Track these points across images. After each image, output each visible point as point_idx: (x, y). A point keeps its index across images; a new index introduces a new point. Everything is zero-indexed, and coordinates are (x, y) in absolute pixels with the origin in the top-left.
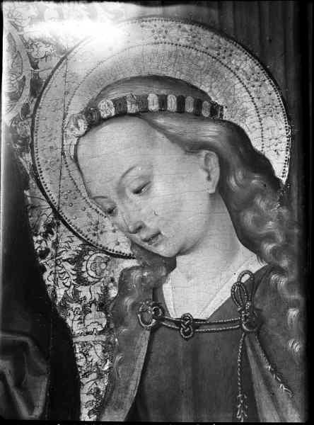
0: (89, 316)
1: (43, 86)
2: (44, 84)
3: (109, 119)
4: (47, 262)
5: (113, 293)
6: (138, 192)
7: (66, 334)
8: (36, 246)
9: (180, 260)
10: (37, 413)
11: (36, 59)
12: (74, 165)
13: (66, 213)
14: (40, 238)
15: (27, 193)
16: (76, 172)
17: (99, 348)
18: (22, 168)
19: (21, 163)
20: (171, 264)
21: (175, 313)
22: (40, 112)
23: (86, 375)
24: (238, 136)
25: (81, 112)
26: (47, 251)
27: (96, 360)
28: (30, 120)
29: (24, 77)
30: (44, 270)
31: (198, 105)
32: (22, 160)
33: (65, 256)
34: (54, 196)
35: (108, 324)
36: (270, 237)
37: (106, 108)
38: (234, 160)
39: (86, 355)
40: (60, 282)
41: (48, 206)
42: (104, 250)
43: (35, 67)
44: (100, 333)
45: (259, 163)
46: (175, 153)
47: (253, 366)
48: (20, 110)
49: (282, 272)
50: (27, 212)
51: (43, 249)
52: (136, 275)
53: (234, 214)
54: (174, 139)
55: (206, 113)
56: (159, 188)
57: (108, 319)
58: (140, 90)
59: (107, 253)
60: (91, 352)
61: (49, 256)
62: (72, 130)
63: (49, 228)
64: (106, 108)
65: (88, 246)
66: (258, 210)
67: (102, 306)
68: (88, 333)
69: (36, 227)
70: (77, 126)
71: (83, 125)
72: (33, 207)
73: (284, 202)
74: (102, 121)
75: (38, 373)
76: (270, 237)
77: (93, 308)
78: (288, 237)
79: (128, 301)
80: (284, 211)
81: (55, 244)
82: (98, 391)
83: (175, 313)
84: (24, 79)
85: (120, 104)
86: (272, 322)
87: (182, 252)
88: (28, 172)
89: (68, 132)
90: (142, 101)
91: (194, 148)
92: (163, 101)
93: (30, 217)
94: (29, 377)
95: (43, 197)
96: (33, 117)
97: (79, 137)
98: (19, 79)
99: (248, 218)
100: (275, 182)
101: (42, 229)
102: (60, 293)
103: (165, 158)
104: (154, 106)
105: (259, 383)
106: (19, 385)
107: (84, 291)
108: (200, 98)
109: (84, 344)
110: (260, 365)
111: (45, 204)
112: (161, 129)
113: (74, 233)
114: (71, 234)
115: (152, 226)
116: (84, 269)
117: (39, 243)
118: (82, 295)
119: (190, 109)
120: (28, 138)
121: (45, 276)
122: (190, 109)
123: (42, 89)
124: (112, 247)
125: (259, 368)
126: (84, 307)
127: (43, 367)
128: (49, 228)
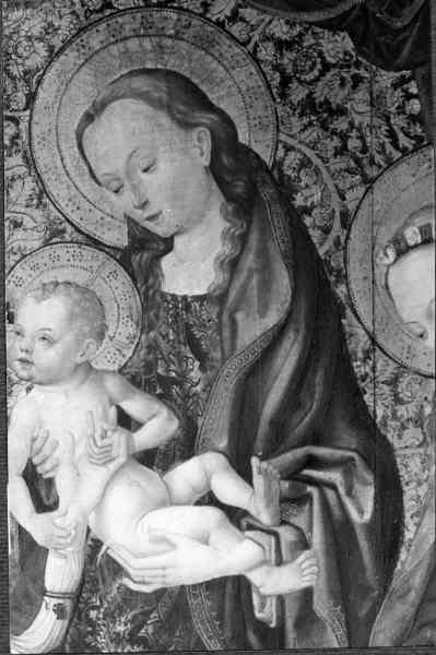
0: (407, 431)
3: (416, 246)
4: (366, 385)
7: (388, 448)
8: (356, 370)
10: (368, 516)
12: (385, 292)
13: (380, 340)
14: (359, 363)
15: (344, 321)
16: (389, 300)
17: (418, 460)
22: (350, 243)
23: (407, 484)
25: (389, 242)
26: (367, 375)
27: (416, 470)
30: (365, 392)
32: (338, 291)
33: (381, 379)
34: (369, 324)
35: (425, 438)
37: (412, 235)
39: (406, 466)
40: (379, 402)
42: (417, 373)
44: (419, 446)
48: (332, 243)
50: (345, 341)
57: (424, 434)
59: (421, 375)
60: (411, 464)
61: (369, 380)
62: (381, 259)
63: (367, 355)
64: (412, 235)
68: (406, 447)
69: (356, 354)
70: (386, 255)
71: (391, 253)
72: (351, 335)
74: (409, 248)
75: (366, 484)
77: (411, 425)
81: (374, 369)
82: (419, 497)
84: (333, 211)
88: (344, 302)
89: (378, 261)
94: (357, 487)
96: (345, 248)
97: (389, 266)
101: (360, 355)
102: (380, 413)
106: (349, 493)
107: (402, 411)
109: (405, 456)
113: (390, 358)
114: (386, 358)
116: (399, 390)
117: (360, 369)
118: (399, 414)
121: (366, 397)
126: (402, 424)
127: (370, 478)
128: (367, 357)
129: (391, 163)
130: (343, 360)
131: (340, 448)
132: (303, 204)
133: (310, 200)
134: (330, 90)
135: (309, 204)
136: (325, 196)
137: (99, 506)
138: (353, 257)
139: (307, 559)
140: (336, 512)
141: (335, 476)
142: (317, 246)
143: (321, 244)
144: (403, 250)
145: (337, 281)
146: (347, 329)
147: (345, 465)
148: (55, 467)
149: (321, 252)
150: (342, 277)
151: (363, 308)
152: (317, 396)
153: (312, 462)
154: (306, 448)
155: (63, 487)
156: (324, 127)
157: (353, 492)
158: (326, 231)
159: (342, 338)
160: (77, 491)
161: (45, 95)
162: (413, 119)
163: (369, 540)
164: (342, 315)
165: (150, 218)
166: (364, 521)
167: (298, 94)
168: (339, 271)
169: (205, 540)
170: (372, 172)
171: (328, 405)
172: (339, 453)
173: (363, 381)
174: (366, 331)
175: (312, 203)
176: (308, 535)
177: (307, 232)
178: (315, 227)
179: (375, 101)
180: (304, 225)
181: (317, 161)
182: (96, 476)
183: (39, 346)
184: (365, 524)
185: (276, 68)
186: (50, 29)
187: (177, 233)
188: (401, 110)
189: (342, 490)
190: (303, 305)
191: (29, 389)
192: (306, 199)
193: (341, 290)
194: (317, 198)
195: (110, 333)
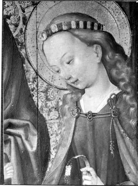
0: (51, 112)
1: (28, 20)
2: (28, 19)
3: (56, 32)
4: (34, 93)
5: (61, 103)
6: (69, 63)
7: (44, 120)
8: (30, 86)
9: (86, 90)
10: (35, 149)
11: (24, 8)
12: (42, 53)
13: (40, 73)
14: (31, 83)
15: (24, 65)
16: (44, 56)
17: (56, 125)
18: (22, 55)
19: (21, 53)
20: (83, 92)
21: (85, 110)
22: (27, 31)
23: (52, 135)
24: (110, 37)
25: (44, 30)
26: (34, 88)
27: (55, 129)
28: (23, 35)
29: (19, 16)
31: (92, 25)
32: (21, 52)
33: (41, 90)
34: (35, 66)
35: (59, 116)
36: (123, 80)
37: (54, 28)
38: (108, 48)
39: (51, 128)
40: (39, 100)
41: (33, 70)
42: (56, 87)
43: (24, 12)
44: (57, 119)
45: (118, 49)
46: (84, 46)
47: (117, 130)
48: (19, 31)
49: (128, 93)
50: (25, 73)
51: (32, 88)
52: (69, 97)
53: (108, 71)
54: (83, 40)
55: (96, 28)
56: (77, 61)
57: (59, 114)
58: (67, 19)
59: (58, 88)
60: (53, 127)
61: (35, 91)
62: (41, 38)
64: (54, 28)
65: (50, 85)
66: (118, 69)
67: (56, 109)
68: (51, 119)
69: (29, 79)
70: (42, 36)
71: (45, 36)
72: (27, 71)
73: (130, 65)
74: (52, 34)
75: (34, 135)
76: (123, 80)
77: (53, 110)
78: (130, 80)
79: (67, 107)
80: (129, 69)
81: (37, 86)
82: (57, 141)
83: (85, 110)
84: (19, 17)
85: (59, 26)
86: (124, 113)
87: (87, 87)
88: (24, 57)
89: (39, 39)
90: (69, 24)
91: (91, 43)
92: (78, 24)
93: (27, 75)
94: (30, 136)
95: (31, 67)
96: (25, 33)
97: (44, 41)
98: (17, 17)
99: (114, 72)
100: (125, 57)
101: (31, 80)
102: (40, 104)
103: (79, 48)
104: (74, 26)
105: (118, 136)
107: (49, 103)
108: (93, 21)
109: (51, 123)
110: (119, 130)
111: (32, 70)
112: (77, 36)
113: (44, 81)
114: (43, 81)
115: (74, 77)
116: (48, 95)
117: (31, 85)
118: (48, 105)
119: (89, 27)
120: (23, 43)
121: (34, 98)
122: (89, 27)
123: (27, 21)
124: (59, 86)
125: (119, 131)
126: (50, 110)
127: (35, 132)
130: (24, 81)
131: (23, 120)
132: (6, 14)
133: (10, 12)
135: (9, 14)
136: (16, 11)
138: (28, 38)
139: (9, 166)
140: (21, 147)
141: (20, 132)
142: (13, 33)
143: (14, 32)
144: (50, 34)
145: (21, 48)
146: (25, 68)
147: (25, 127)
149: (14, 35)
150: (23, 46)
151: (32, 59)
152: (13, 97)
153: (11, 125)
154: (8, 120)
157: (28, 139)
158: (16, 26)
159: (24, 72)
163: (35, 159)
164: (23, 62)
166: (33, 151)
168: (22, 44)
171: (17, 102)
172: (22, 122)
173: (33, 91)
174: (34, 69)
175: (10, 14)
176: (9, 156)
177: (8, 26)
178: (11, 24)
180: (7, 23)
184: (33, 152)
189: (23, 138)
190: (6, 59)
192: (8, 12)
193: (23, 52)
194: (12, 12)
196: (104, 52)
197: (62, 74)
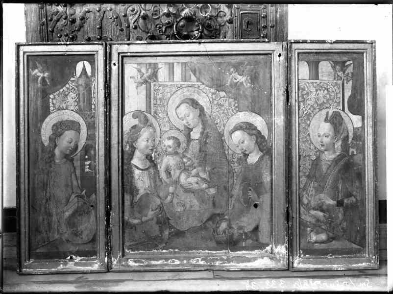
24: (259, 132)
36: (265, 150)
45: (263, 137)
56: (246, 142)
65: (234, 152)
76: (265, 150)
103: (246, 136)
115: (244, 148)
129: (233, 115)
134: (221, 102)
136: (220, 121)
137: (179, 177)
148: (171, 170)
155: (172, 172)
156: (220, 108)
158: (220, 127)
160: (175, 173)
161: (170, 102)
162: (236, 107)
165: (189, 125)
167: (216, 102)
169: (197, 183)
170: (229, 117)
179: (230, 104)
181: (219, 115)
182: (178, 172)
183: (168, 148)
185: (211, 98)
186: (171, 91)
187: (194, 127)
188: (234, 105)
191: (166, 156)
195: (181, 146)
196: (257, 138)
197: (240, 148)
